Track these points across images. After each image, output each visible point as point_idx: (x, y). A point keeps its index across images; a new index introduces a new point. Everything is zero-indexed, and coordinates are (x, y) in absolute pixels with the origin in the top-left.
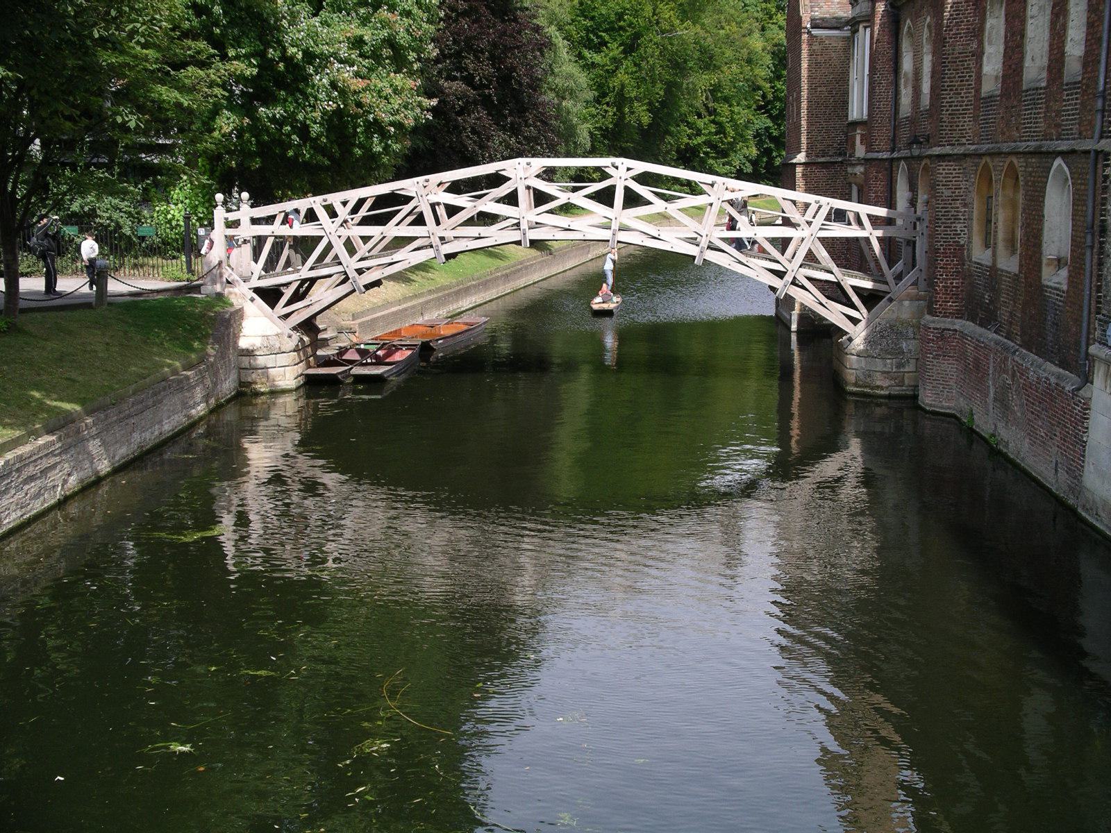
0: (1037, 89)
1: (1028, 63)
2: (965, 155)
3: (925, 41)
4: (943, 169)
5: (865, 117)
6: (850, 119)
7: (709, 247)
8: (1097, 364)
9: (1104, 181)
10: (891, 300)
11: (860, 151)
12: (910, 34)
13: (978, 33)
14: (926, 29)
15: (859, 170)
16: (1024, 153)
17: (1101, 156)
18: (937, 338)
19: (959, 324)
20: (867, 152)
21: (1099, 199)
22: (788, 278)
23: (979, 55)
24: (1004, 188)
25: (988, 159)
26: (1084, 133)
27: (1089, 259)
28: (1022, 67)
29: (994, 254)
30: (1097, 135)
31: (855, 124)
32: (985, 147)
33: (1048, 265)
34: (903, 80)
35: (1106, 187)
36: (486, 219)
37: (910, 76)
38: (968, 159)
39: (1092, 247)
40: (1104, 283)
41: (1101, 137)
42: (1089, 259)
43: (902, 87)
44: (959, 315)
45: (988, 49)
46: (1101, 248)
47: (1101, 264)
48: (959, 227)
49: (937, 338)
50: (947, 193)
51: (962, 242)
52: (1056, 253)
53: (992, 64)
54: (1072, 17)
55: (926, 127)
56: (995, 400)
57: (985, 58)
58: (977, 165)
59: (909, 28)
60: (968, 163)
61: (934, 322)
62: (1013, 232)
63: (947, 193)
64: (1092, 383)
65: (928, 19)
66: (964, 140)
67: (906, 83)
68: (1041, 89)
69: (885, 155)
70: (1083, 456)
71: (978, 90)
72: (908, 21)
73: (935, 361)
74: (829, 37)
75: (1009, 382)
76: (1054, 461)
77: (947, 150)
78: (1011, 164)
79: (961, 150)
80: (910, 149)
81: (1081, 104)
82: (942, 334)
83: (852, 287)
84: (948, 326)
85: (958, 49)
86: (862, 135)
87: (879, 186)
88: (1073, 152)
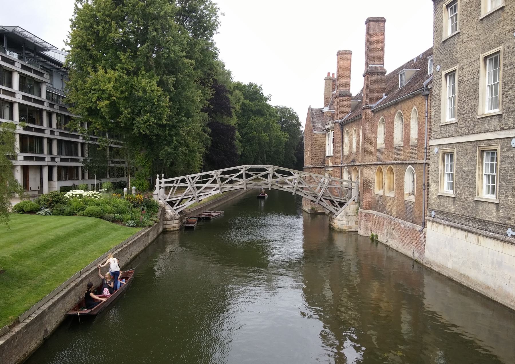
0: (399, 147)
1: (395, 140)
2: (372, 165)
4: (365, 169)
5: (333, 155)
6: (326, 155)
7: (296, 191)
8: (428, 222)
9: (428, 172)
10: (348, 205)
11: (330, 164)
12: (348, 133)
13: (376, 131)
14: (354, 131)
15: (330, 169)
16: (396, 164)
17: (427, 165)
19: (371, 212)
20: (333, 164)
21: (427, 176)
22: (319, 199)
23: (376, 138)
25: (381, 166)
26: (419, 159)
27: (424, 193)
28: (393, 141)
29: (384, 192)
30: (425, 159)
31: (328, 157)
32: (380, 163)
33: (406, 195)
34: (345, 145)
35: (429, 173)
36: (231, 182)
37: (348, 144)
38: (373, 166)
39: (425, 189)
40: (429, 200)
41: (426, 160)
42: (424, 193)
43: (345, 147)
44: (371, 209)
45: (378, 136)
46: (428, 190)
47: (428, 194)
48: (370, 185)
50: (366, 175)
51: (371, 189)
52: (408, 191)
53: (381, 141)
54: (411, 128)
55: (356, 158)
56: (387, 233)
57: (378, 138)
58: (376, 168)
59: (347, 131)
60: (373, 167)
61: (363, 211)
62: (390, 186)
63: (366, 175)
64: (426, 227)
65: (355, 128)
66: (371, 161)
68: (401, 147)
69: (340, 165)
70: (425, 248)
71: (375, 147)
72: (347, 129)
75: (393, 227)
76: (412, 250)
77: (366, 163)
78: (390, 167)
79: (371, 163)
80: (351, 163)
81: (418, 150)
82: (366, 214)
83: (337, 201)
86: (331, 160)
87: (338, 174)
88: (416, 163)
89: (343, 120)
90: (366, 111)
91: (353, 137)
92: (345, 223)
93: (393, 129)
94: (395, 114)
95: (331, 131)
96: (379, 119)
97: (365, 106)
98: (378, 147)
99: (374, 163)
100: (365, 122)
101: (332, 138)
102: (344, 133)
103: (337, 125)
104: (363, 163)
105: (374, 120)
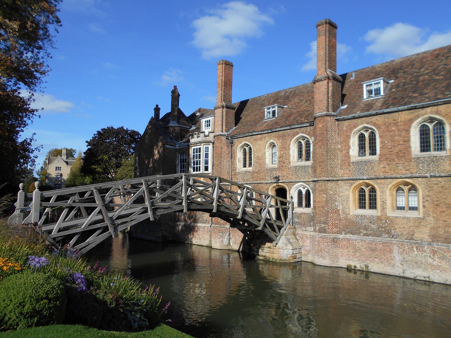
1: (413, 149)
3: (267, 147)
18: (332, 241)
19: (341, 236)
24: (390, 189)
32: (365, 178)
34: (237, 160)
38: (340, 182)
43: (237, 162)
44: (339, 233)
48: (337, 204)
49: (332, 241)
50: (331, 192)
51: (338, 208)
57: (351, 150)
63: (331, 192)
66: (337, 176)
67: (239, 161)
73: (331, 249)
74: (170, 148)
77: (331, 178)
79: (338, 179)
84: (336, 237)
85: (333, 147)
89: (229, 133)
90: (328, 118)
91: (266, 150)
92: (291, 252)
93: (409, 137)
94: (411, 121)
95: (204, 145)
96: (355, 127)
97: (325, 113)
98: (353, 159)
99: (344, 178)
100: (327, 130)
101: (204, 153)
102: (234, 148)
103: (224, 139)
104: (327, 179)
105: (338, 130)
